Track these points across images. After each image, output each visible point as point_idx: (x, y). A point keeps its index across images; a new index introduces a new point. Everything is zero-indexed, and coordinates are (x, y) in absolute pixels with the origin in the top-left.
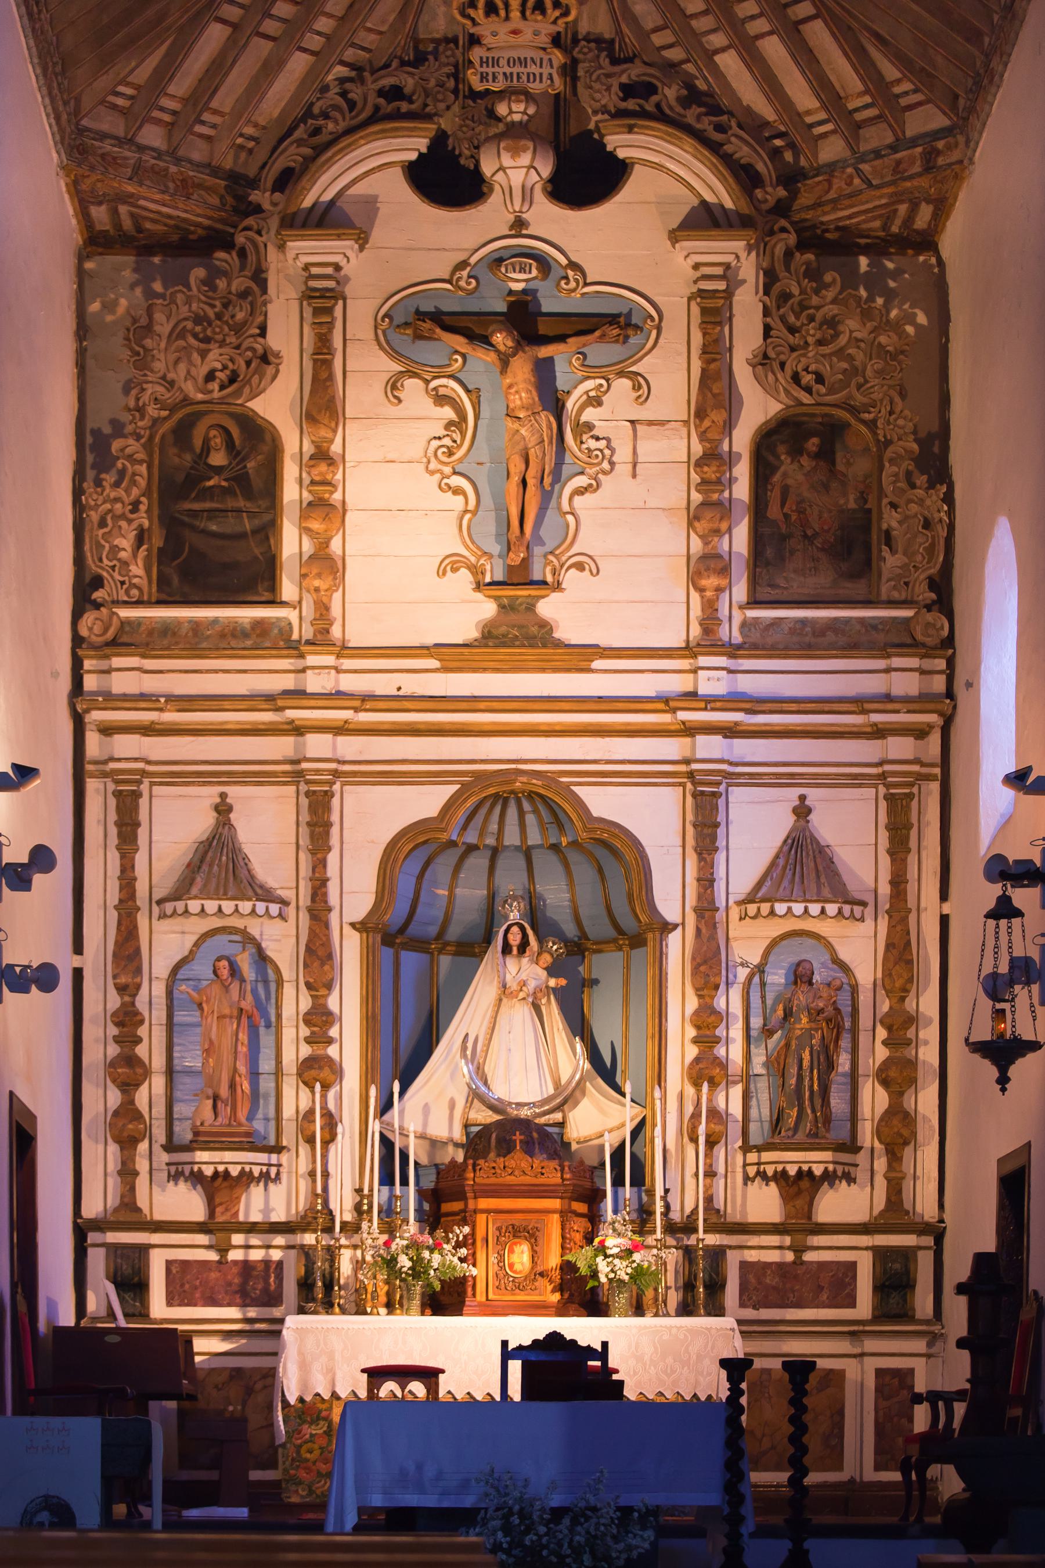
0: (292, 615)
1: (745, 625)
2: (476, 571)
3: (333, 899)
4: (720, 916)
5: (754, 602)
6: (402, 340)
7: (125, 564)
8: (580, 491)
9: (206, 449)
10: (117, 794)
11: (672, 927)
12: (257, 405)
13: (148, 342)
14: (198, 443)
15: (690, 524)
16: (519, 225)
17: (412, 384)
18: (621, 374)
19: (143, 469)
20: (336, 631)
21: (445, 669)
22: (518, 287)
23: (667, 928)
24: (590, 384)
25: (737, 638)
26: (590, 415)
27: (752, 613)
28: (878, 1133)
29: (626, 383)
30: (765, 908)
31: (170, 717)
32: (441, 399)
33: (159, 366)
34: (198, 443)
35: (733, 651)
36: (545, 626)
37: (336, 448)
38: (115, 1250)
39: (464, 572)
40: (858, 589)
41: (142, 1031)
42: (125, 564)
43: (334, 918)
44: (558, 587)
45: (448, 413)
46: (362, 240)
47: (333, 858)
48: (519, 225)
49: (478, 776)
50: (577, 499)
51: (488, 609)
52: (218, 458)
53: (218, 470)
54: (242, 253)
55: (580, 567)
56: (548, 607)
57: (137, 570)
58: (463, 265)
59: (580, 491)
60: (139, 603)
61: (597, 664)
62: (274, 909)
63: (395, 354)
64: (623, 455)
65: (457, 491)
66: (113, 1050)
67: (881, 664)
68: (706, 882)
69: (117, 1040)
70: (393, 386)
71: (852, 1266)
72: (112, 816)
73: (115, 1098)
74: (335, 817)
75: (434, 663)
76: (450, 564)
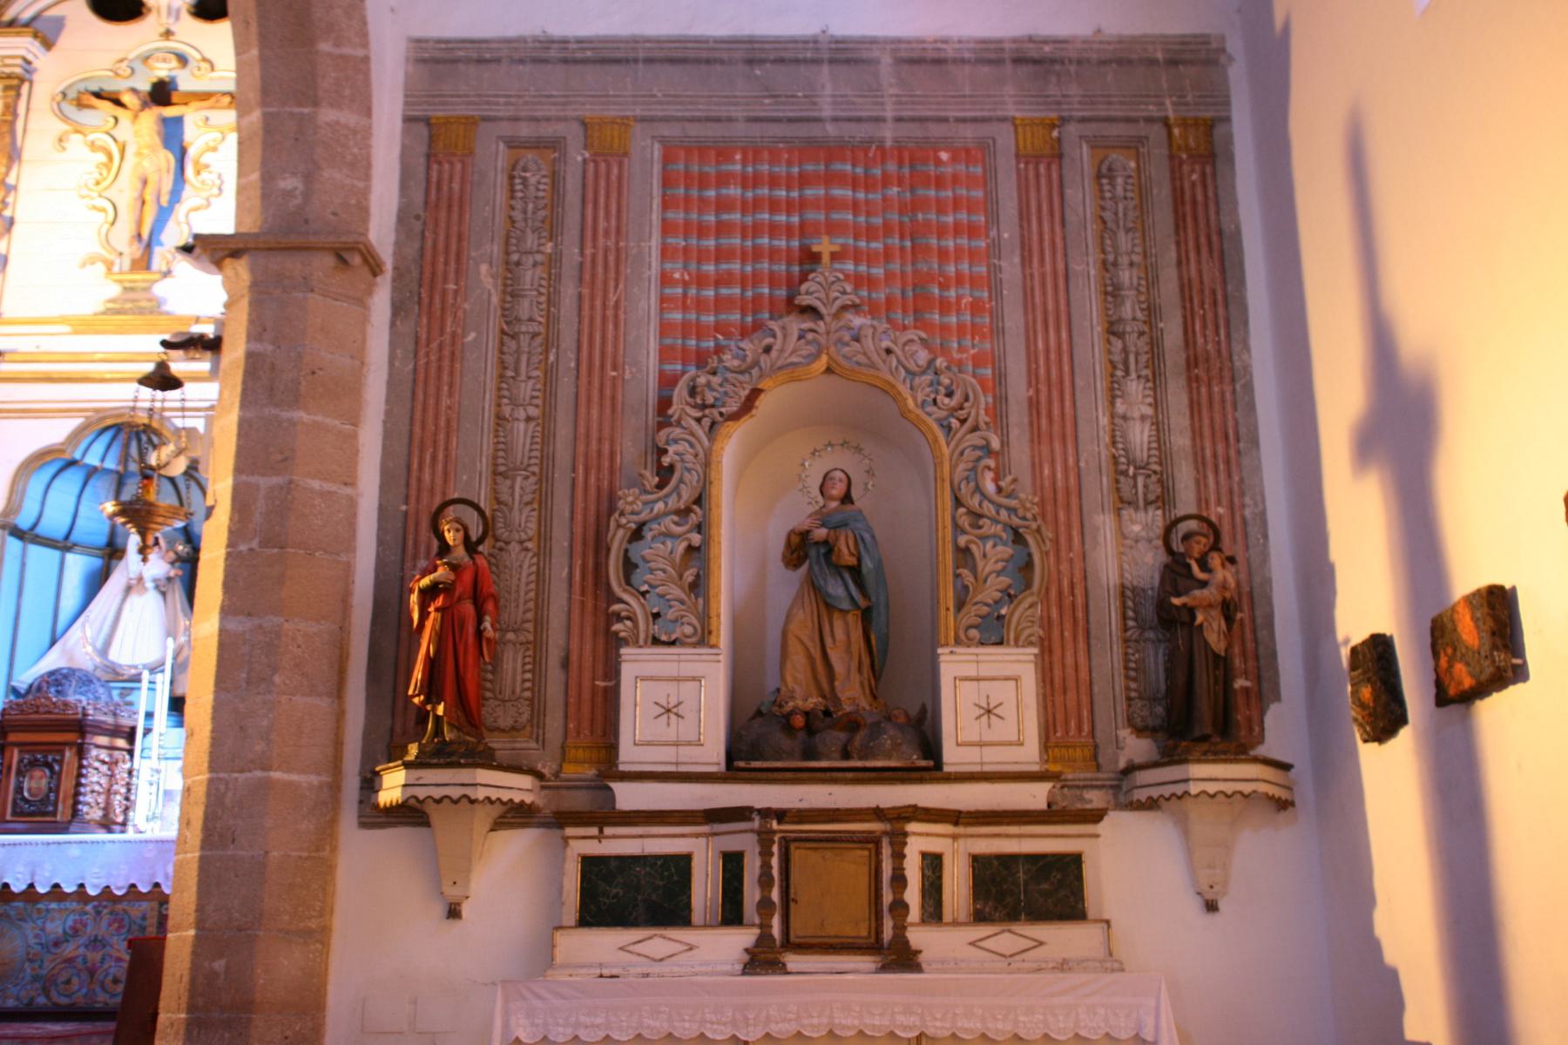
2: (109, 266)
6: (69, 109)
8: (196, 209)
21: (76, 332)
26: (206, 159)
32: (93, 146)
44: (167, 274)
46: (48, 44)
49: (97, 411)
50: (193, 215)
51: (115, 290)
56: (160, 289)
63: (65, 118)
65: (104, 210)
75: (66, 329)
76: (91, 260)
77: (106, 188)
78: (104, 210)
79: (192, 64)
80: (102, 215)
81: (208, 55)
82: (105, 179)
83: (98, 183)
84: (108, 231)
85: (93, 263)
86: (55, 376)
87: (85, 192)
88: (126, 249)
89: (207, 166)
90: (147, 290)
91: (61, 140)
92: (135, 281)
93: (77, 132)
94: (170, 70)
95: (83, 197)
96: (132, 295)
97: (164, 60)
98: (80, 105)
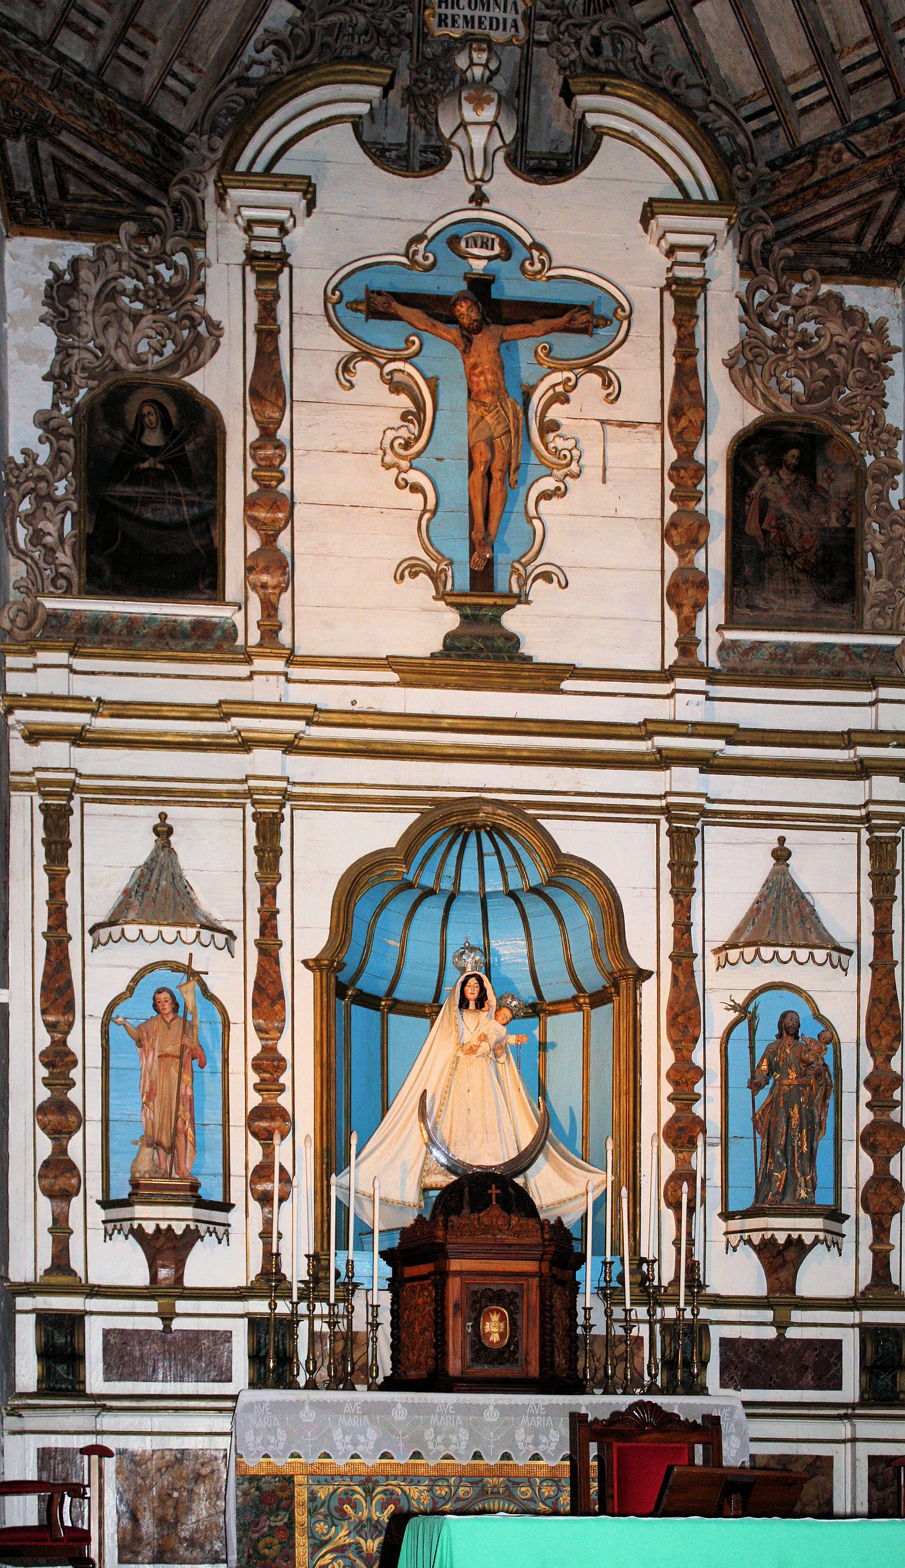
0: (239, 619)
1: (725, 648)
3: (283, 933)
4: (697, 964)
5: (731, 623)
6: (356, 321)
7: (50, 551)
8: (546, 495)
9: (140, 426)
10: (45, 809)
11: (650, 974)
12: (196, 381)
13: (74, 302)
14: (131, 419)
15: (666, 535)
16: (479, 198)
17: (365, 370)
18: (590, 368)
19: (70, 444)
20: (284, 636)
22: (478, 266)
23: (643, 975)
24: (557, 377)
25: (715, 663)
26: (556, 412)
27: (731, 635)
28: (865, 1202)
29: (594, 379)
30: (749, 952)
31: (102, 723)
32: (396, 388)
33: (86, 329)
34: (131, 419)
35: (712, 677)
36: (513, 640)
37: (282, 434)
38: (45, 1319)
39: (423, 577)
40: (843, 613)
41: (75, 1074)
42: (50, 551)
43: (284, 954)
44: (522, 598)
45: (404, 402)
47: (283, 889)
48: (479, 198)
49: (438, 803)
50: (543, 503)
51: (451, 620)
52: (153, 438)
53: (154, 451)
54: (177, 209)
55: (547, 577)
56: (512, 621)
57: (64, 557)
58: (418, 239)
59: (546, 495)
60: (67, 593)
61: (566, 685)
62: (220, 938)
63: (345, 334)
64: (591, 458)
65: (416, 488)
66: (44, 1094)
67: (867, 696)
68: (683, 927)
69: (47, 1083)
70: (346, 366)
71: (837, 1345)
72: (40, 833)
73: (46, 1147)
74: (284, 843)
75: (394, 677)
77: (419, 454)
78: (416, 488)
79: (519, 253)
80: (420, 496)
81: (539, 240)
82: (417, 439)
83: (407, 445)
84: (429, 520)
85: (414, 575)
86: (379, 747)
87: (389, 458)
88: (460, 551)
89: (554, 426)
90: (496, 620)
91: (346, 369)
92: (482, 606)
93: (367, 356)
94: (490, 259)
95: (388, 467)
96: (478, 630)
97: (484, 245)
98: (374, 313)
